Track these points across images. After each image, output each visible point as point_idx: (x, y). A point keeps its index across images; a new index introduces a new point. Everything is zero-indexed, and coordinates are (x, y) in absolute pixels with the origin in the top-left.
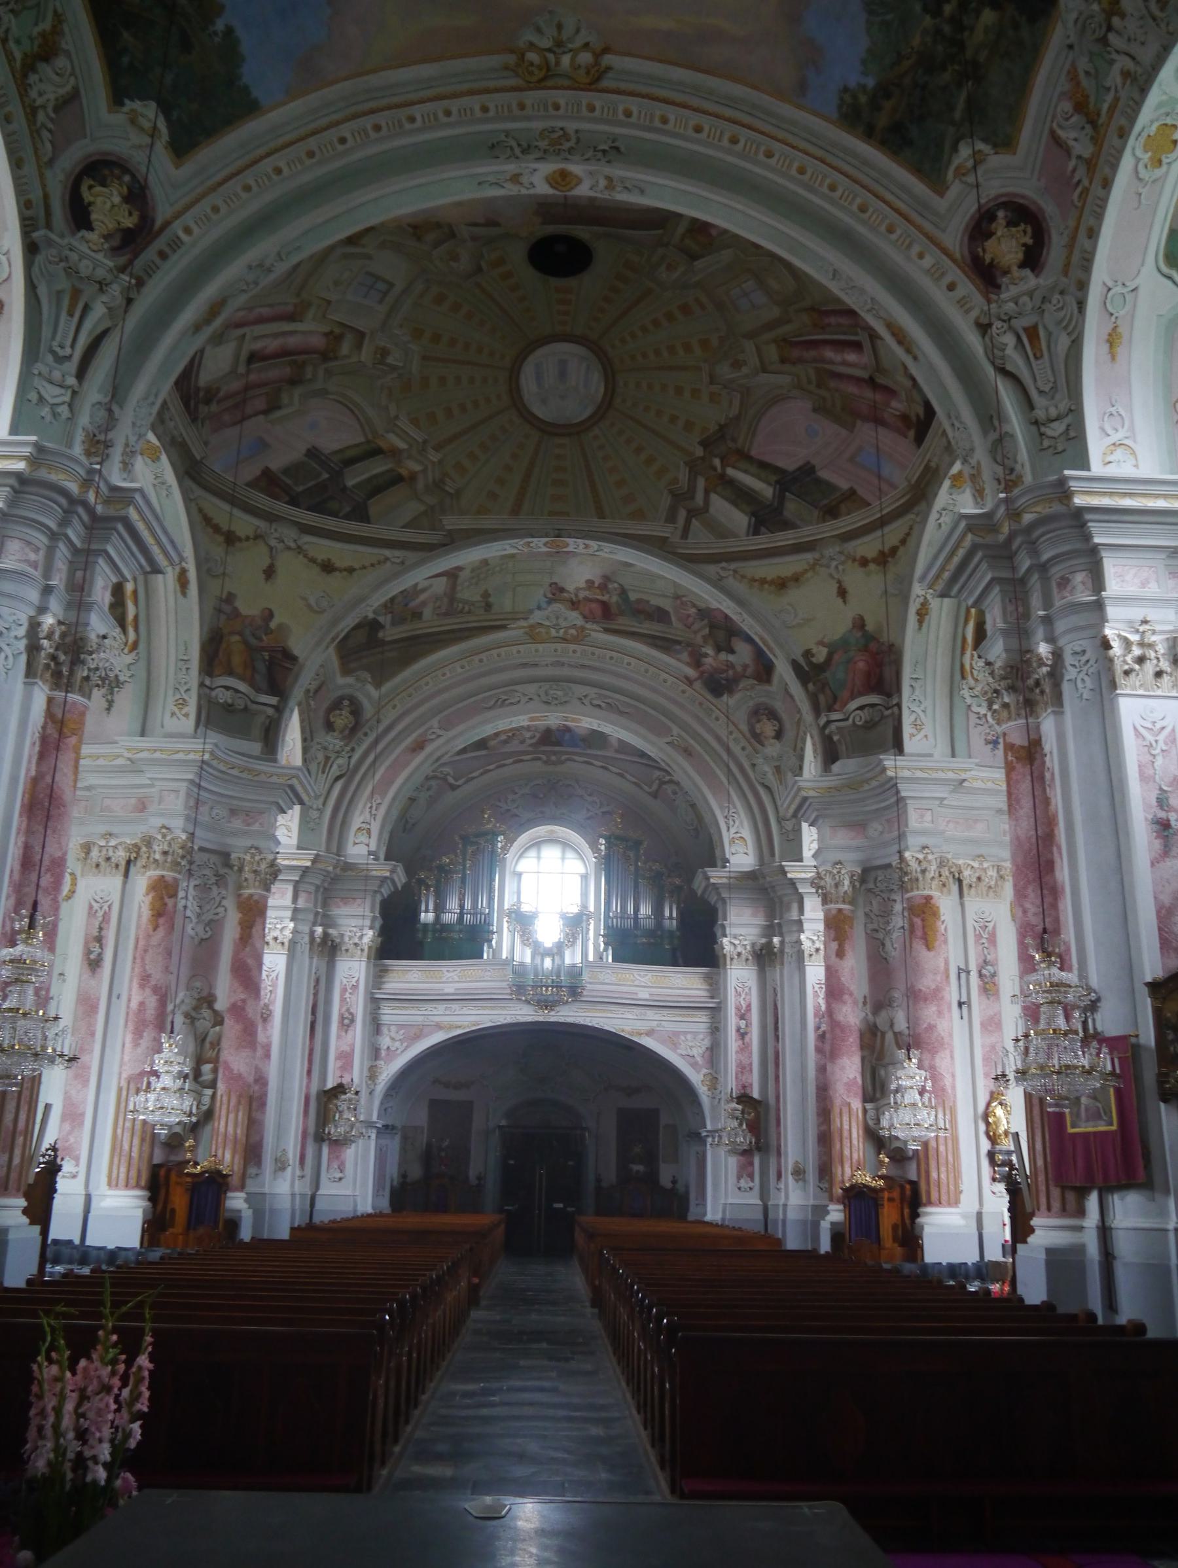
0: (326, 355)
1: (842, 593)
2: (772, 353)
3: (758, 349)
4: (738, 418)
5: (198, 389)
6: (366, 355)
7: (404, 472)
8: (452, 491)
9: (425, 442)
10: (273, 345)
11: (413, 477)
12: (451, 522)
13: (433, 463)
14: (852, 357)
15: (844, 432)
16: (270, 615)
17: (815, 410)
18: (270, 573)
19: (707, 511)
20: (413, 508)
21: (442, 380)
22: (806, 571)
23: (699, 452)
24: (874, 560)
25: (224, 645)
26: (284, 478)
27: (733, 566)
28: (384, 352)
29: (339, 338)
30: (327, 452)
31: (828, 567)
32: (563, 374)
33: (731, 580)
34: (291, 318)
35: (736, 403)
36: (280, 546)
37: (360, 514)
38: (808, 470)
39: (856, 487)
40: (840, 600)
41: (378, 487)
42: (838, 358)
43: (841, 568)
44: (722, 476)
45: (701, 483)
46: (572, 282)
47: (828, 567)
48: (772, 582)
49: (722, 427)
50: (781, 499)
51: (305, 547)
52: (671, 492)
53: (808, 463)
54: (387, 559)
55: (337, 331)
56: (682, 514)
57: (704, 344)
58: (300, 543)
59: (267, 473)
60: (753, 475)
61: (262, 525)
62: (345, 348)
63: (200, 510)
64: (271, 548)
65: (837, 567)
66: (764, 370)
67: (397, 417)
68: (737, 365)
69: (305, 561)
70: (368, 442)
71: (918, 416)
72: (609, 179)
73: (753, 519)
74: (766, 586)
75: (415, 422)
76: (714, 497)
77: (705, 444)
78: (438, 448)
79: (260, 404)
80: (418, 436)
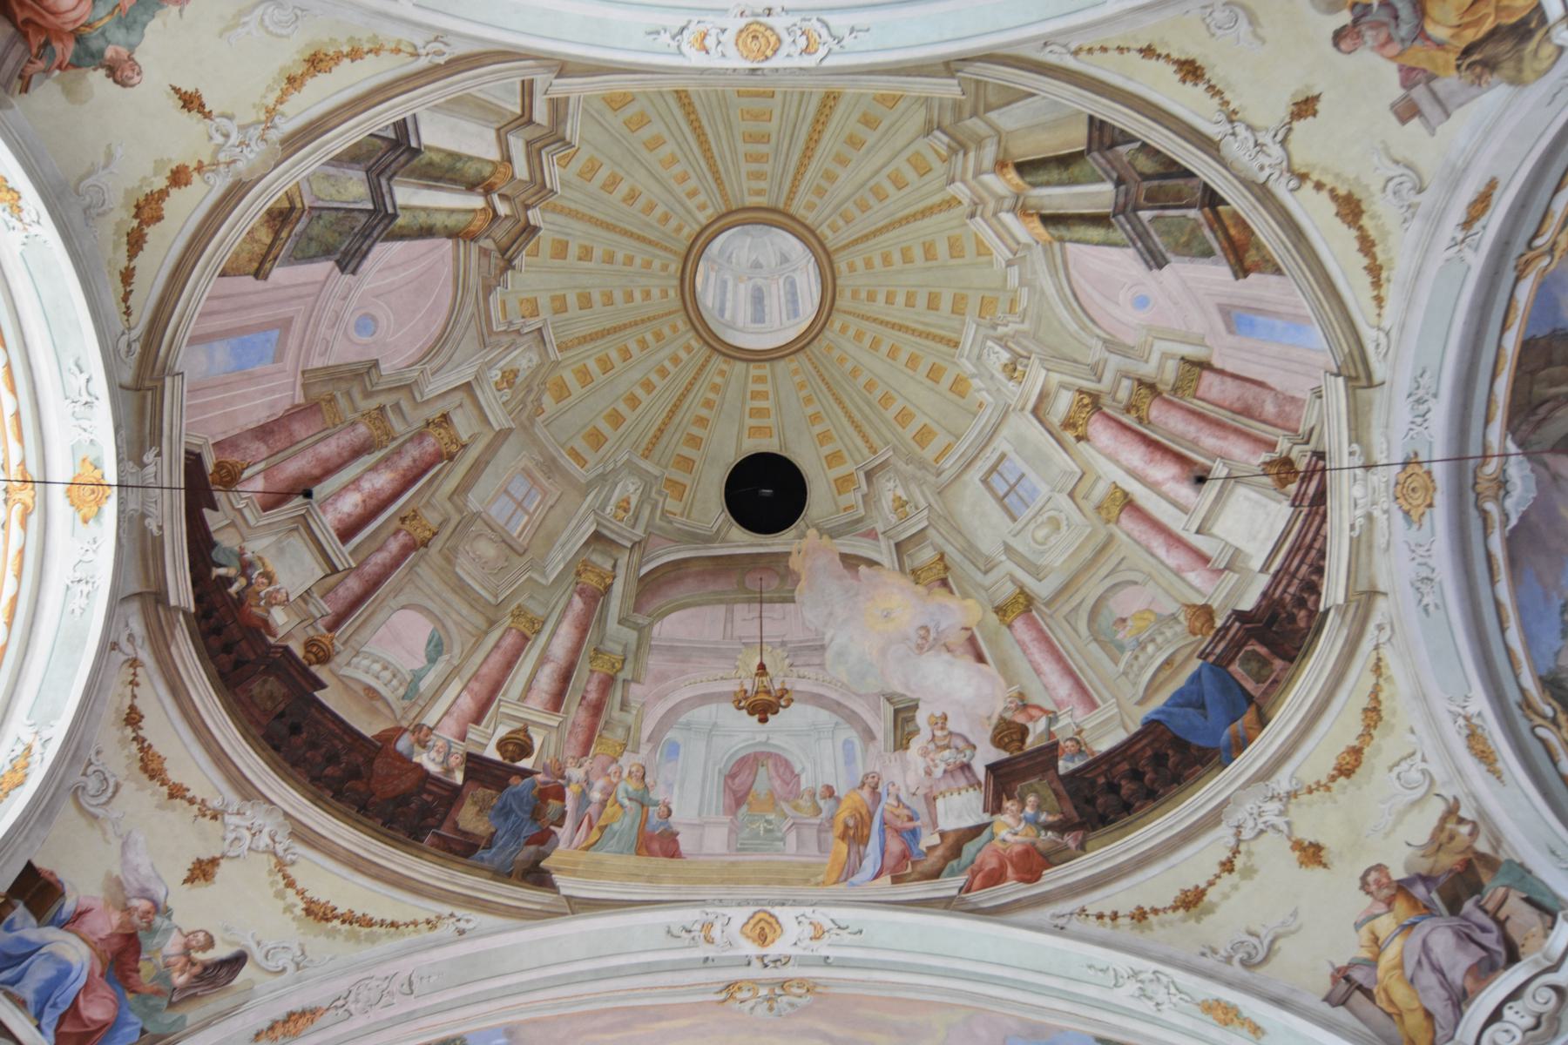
0: (1094, 403)
1: (190, 102)
2: (463, 425)
3: (485, 420)
4: (488, 290)
5: (1296, 502)
6: (1037, 377)
7: (1012, 175)
8: (937, 133)
9: (972, 215)
10: (1164, 472)
11: (1000, 165)
12: (948, 89)
13: (963, 181)
14: (350, 504)
15: (317, 363)
16: (1338, 37)
17: (375, 364)
18: (1305, 107)
19: (498, 130)
20: (1007, 119)
21: (933, 303)
22: (280, 101)
23: (534, 216)
24: (163, 194)
25: (1470, 35)
26: (1216, 246)
27: (423, 63)
28: (1011, 369)
29: (1069, 424)
30: (1131, 251)
31: (243, 128)
32: (758, 298)
33: (419, 42)
34: (1129, 504)
35: (496, 313)
36: (1265, 138)
37: (1102, 135)
38: (349, 261)
39: (260, 284)
40: (188, 87)
41: (1064, 164)
42: (366, 485)
43: (219, 139)
44: (488, 191)
45: (521, 169)
46: (752, 446)
47: (243, 128)
48: (338, 57)
49: (509, 265)
50: (376, 194)
51: (1223, 117)
52: (569, 145)
53: (354, 272)
54: (1076, 53)
55: (1069, 436)
56: (541, 114)
57: (562, 392)
58: (1228, 128)
59: (1241, 269)
60: (437, 210)
61: (1281, 189)
62: (1063, 404)
63: (1379, 300)
64: (1283, 142)
65: (227, 136)
66: (468, 387)
67: (1009, 264)
68: (510, 377)
69: (1228, 96)
70: (1062, 240)
71: (214, 507)
72: (709, 940)
73: (414, 144)
74: (346, 49)
75: (982, 249)
76: (494, 154)
77: (530, 230)
78: (951, 203)
79: (1210, 385)
80: (979, 225)
